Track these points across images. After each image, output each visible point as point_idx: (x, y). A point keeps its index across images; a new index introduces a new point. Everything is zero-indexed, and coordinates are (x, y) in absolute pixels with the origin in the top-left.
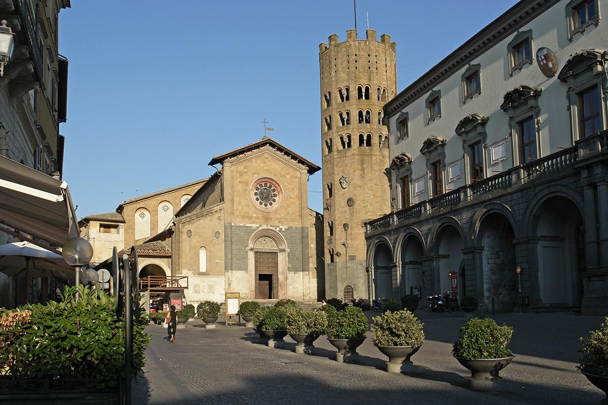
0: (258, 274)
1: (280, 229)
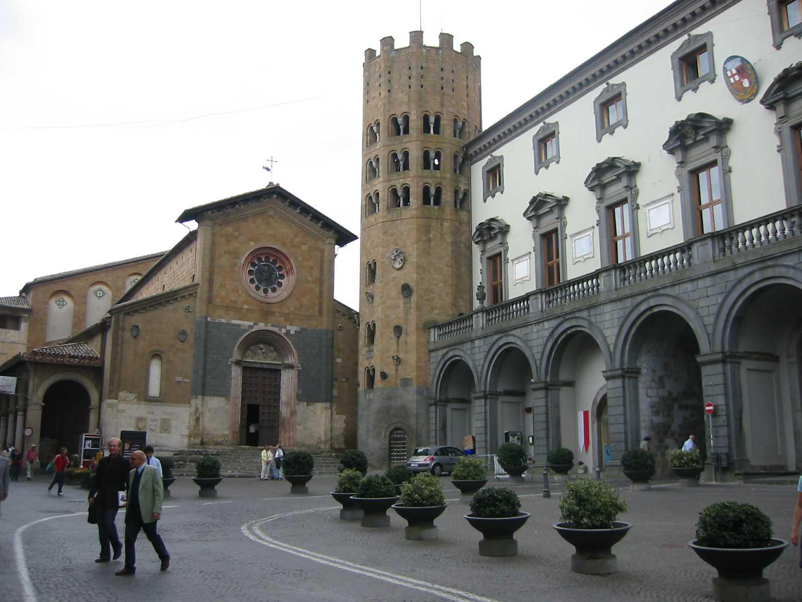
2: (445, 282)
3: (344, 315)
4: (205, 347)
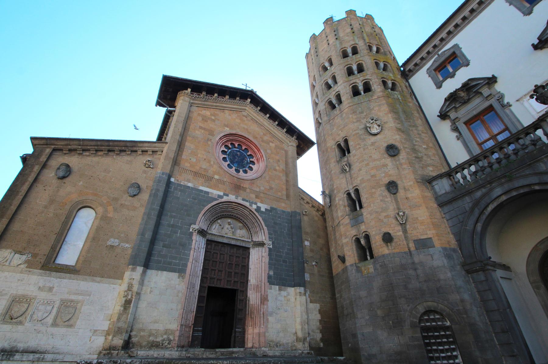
0: (206, 285)
1: (258, 207)
3: (308, 203)
4: (162, 206)
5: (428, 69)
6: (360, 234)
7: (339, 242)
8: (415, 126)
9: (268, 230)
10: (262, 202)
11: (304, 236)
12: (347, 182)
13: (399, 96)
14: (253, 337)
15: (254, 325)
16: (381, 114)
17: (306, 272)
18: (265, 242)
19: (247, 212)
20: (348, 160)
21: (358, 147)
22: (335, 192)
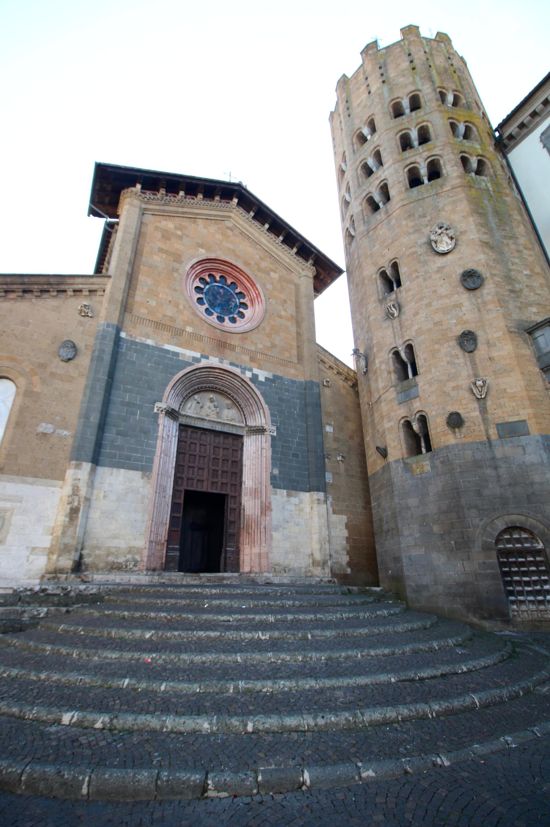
0: (182, 488)
2: (532, 270)
5: (543, 134)
6: (411, 415)
7: (378, 428)
8: (514, 237)
9: (270, 409)
10: (260, 368)
11: (325, 419)
12: (394, 333)
13: (489, 185)
14: (251, 559)
15: (253, 543)
16: (456, 218)
17: (327, 471)
18: (266, 427)
19: (238, 383)
20: (397, 298)
21: (414, 275)
22: (375, 350)
